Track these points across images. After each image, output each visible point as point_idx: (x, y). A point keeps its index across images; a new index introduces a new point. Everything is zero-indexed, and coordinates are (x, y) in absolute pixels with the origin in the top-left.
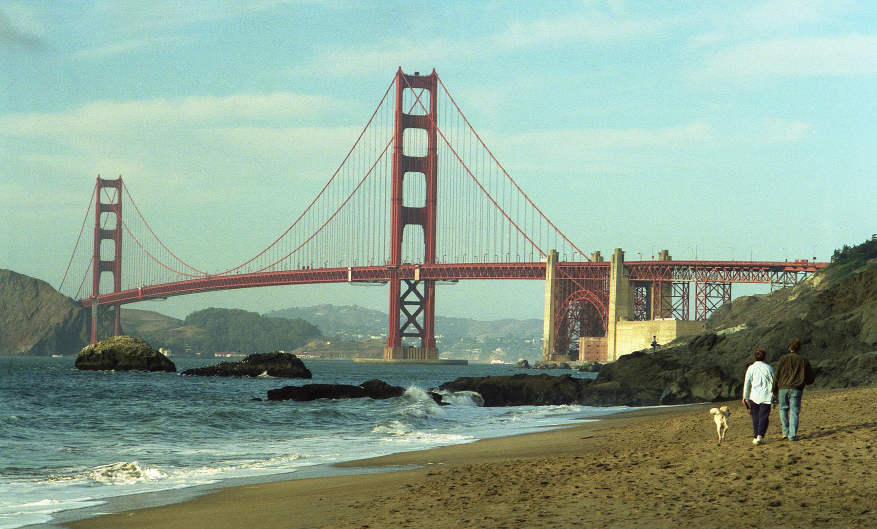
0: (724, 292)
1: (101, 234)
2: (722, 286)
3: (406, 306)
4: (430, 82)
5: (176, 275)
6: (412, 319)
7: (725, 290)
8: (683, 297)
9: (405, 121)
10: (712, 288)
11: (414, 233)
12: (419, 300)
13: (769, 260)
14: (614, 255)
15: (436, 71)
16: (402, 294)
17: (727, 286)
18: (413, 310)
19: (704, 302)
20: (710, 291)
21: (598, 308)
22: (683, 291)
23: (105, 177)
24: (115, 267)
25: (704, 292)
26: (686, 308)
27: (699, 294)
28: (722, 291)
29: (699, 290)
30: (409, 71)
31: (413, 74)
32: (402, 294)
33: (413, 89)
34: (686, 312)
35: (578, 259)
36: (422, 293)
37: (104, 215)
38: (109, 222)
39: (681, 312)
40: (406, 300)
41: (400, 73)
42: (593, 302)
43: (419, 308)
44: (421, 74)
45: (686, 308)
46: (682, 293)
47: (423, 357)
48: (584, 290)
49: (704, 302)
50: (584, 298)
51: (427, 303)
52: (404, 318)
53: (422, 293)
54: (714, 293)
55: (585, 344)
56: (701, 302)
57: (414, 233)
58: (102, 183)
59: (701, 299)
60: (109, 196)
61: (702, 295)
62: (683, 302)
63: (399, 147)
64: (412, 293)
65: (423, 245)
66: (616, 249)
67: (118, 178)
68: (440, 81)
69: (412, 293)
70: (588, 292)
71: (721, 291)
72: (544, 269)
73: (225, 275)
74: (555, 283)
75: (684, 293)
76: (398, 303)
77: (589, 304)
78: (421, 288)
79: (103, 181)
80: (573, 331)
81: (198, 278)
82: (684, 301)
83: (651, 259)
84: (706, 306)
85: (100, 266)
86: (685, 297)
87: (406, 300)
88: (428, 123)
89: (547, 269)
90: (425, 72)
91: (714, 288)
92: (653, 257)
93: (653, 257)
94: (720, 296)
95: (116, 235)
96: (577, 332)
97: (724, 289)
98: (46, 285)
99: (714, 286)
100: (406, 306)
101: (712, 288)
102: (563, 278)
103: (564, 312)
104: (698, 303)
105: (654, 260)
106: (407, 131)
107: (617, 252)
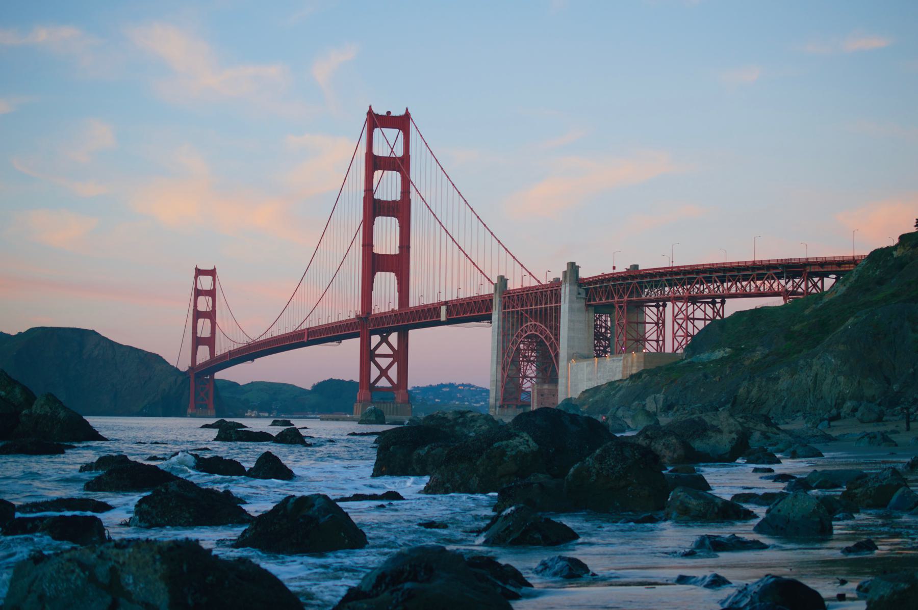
0: (714, 312)
1: (198, 315)
2: (710, 305)
3: (377, 359)
4: (402, 123)
5: (237, 345)
6: (384, 373)
7: (716, 310)
8: (657, 324)
9: (374, 163)
10: (696, 307)
11: (385, 282)
12: (391, 352)
13: (780, 258)
14: (565, 271)
15: (409, 110)
16: (373, 347)
17: (718, 305)
18: (384, 362)
19: (684, 325)
20: (694, 310)
21: (548, 344)
22: (657, 316)
23: (201, 267)
24: (210, 342)
25: (684, 312)
26: (661, 338)
27: (677, 315)
28: (712, 311)
29: (676, 310)
30: (381, 111)
31: (384, 113)
32: (373, 347)
33: (382, 129)
34: (661, 343)
35: (530, 282)
36: (396, 346)
37: (201, 299)
38: (204, 304)
39: (654, 344)
40: (377, 352)
41: (370, 113)
42: (543, 337)
43: (377, 357)
44: (393, 114)
45: (661, 338)
46: (655, 318)
47: (358, 413)
48: (533, 323)
49: (684, 325)
50: (533, 332)
51: (401, 356)
52: (375, 372)
53: (395, 345)
54: (699, 314)
55: (538, 393)
56: (680, 326)
57: (385, 282)
58: (199, 272)
59: (680, 322)
60: (205, 283)
61: (681, 316)
62: (657, 330)
63: (369, 190)
64: (384, 344)
65: (397, 294)
66: (568, 263)
67: (213, 268)
68: (412, 120)
69: (384, 344)
70: (538, 323)
71: (709, 311)
72: (491, 300)
73: (258, 340)
74: (505, 317)
75: (658, 319)
76: (368, 356)
77: (542, 341)
78: (394, 338)
79: (199, 270)
80: (525, 377)
81: (244, 345)
82: (658, 327)
83: (612, 271)
84: (687, 332)
85: (197, 341)
86: (660, 323)
87: (377, 352)
88: (401, 164)
89: (494, 300)
90: (398, 112)
91: (699, 307)
92: (614, 268)
93: (614, 268)
94: (707, 317)
95: (211, 315)
96: (531, 378)
97: (713, 309)
98: (157, 358)
99: (699, 304)
100: (377, 359)
101: (696, 307)
102: (511, 310)
103: (512, 352)
104: (676, 327)
105: (616, 271)
106: (378, 174)
107: (570, 267)
